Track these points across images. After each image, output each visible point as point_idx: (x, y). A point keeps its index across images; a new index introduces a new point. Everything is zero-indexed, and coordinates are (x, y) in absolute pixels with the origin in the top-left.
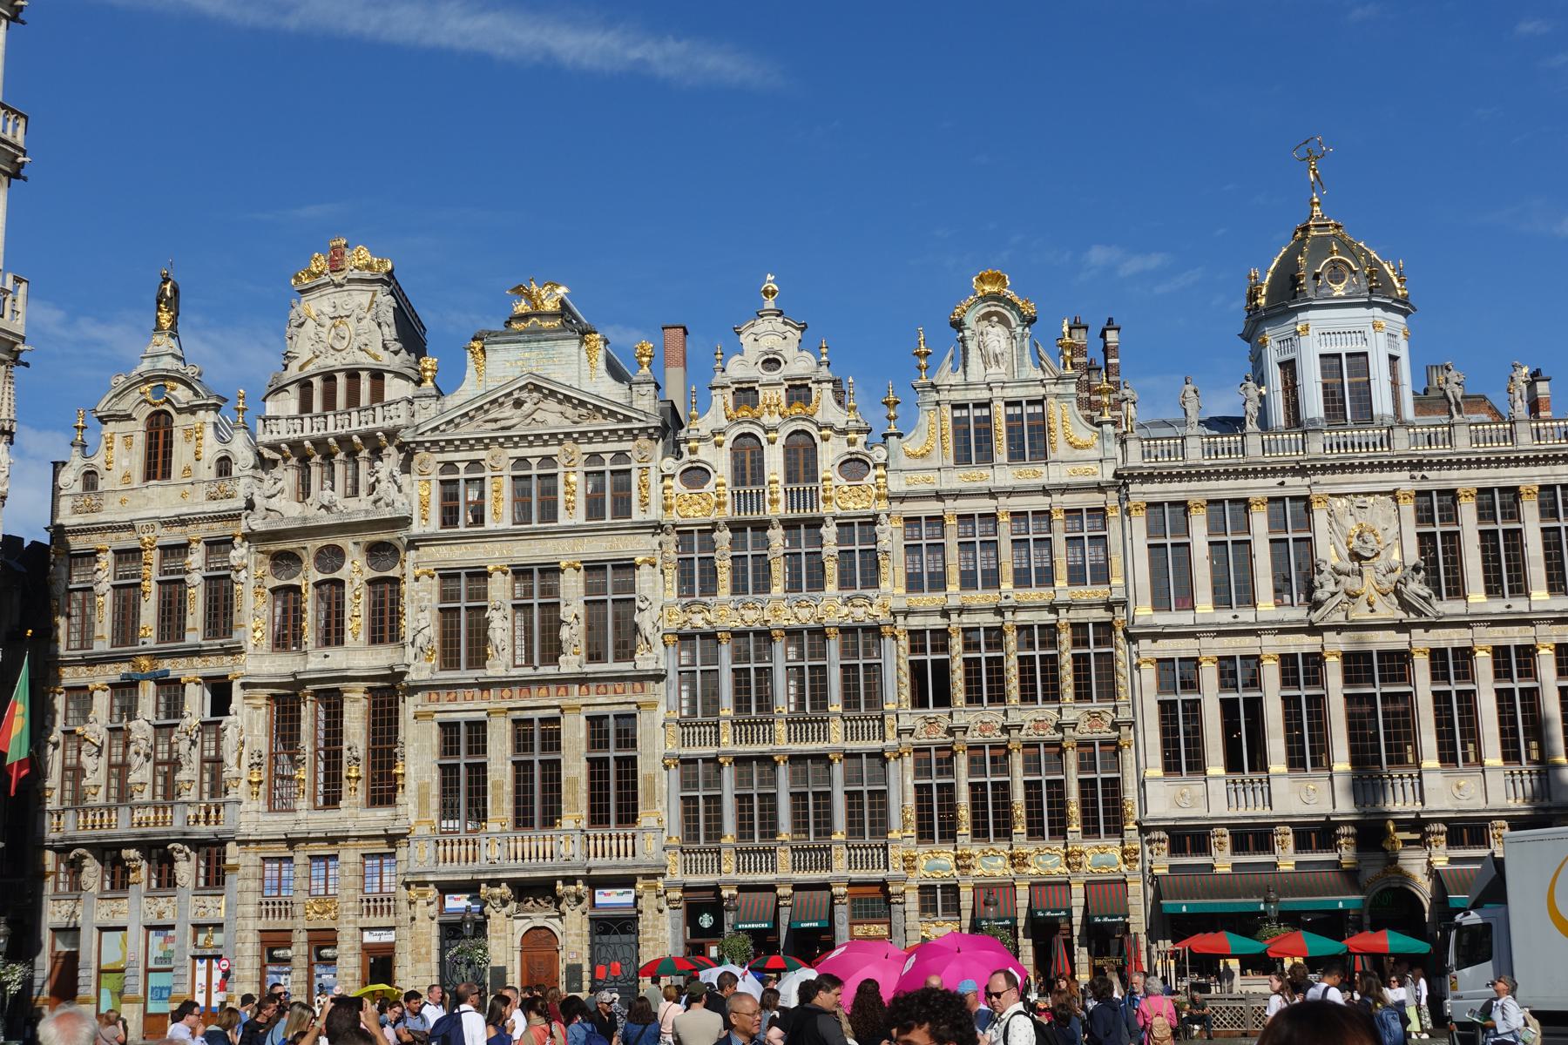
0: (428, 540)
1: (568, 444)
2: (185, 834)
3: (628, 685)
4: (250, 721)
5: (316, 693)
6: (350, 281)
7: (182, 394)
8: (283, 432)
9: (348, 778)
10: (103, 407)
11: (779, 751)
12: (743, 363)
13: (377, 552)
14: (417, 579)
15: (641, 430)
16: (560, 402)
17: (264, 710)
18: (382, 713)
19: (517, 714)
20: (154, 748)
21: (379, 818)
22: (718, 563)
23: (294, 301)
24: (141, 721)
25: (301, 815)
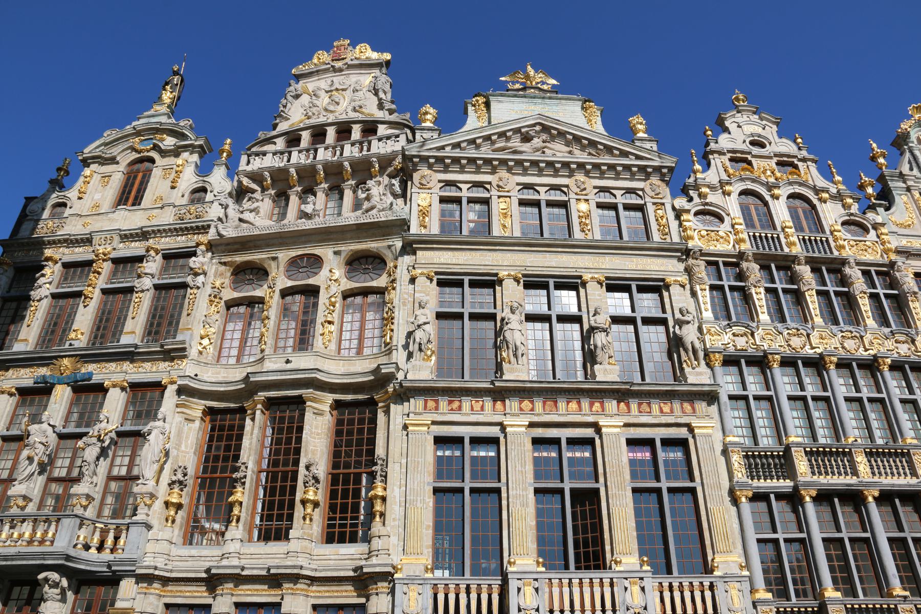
0: (429, 243)
1: (580, 177)
2: (68, 558)
3: (676, 405)
4: (179, 433)
5: (270, 404)
6: (350, 67)
7: (169, 142)
8: (269, 162)
9: (304, 502)
10: (88, 151)
11: (869, 485)
12: (733, 140)
13: (362, 262)
14: (413, 280)
15: (658, 169)
16: (568, 144)
17: (197, 423)
18: (350, 433)
19: (540, 432)
20: (52, 460)
21: (344, 557)
22: (753, 290)
23: (292, 82)
24: (45, 426)
25: (232, 547)
